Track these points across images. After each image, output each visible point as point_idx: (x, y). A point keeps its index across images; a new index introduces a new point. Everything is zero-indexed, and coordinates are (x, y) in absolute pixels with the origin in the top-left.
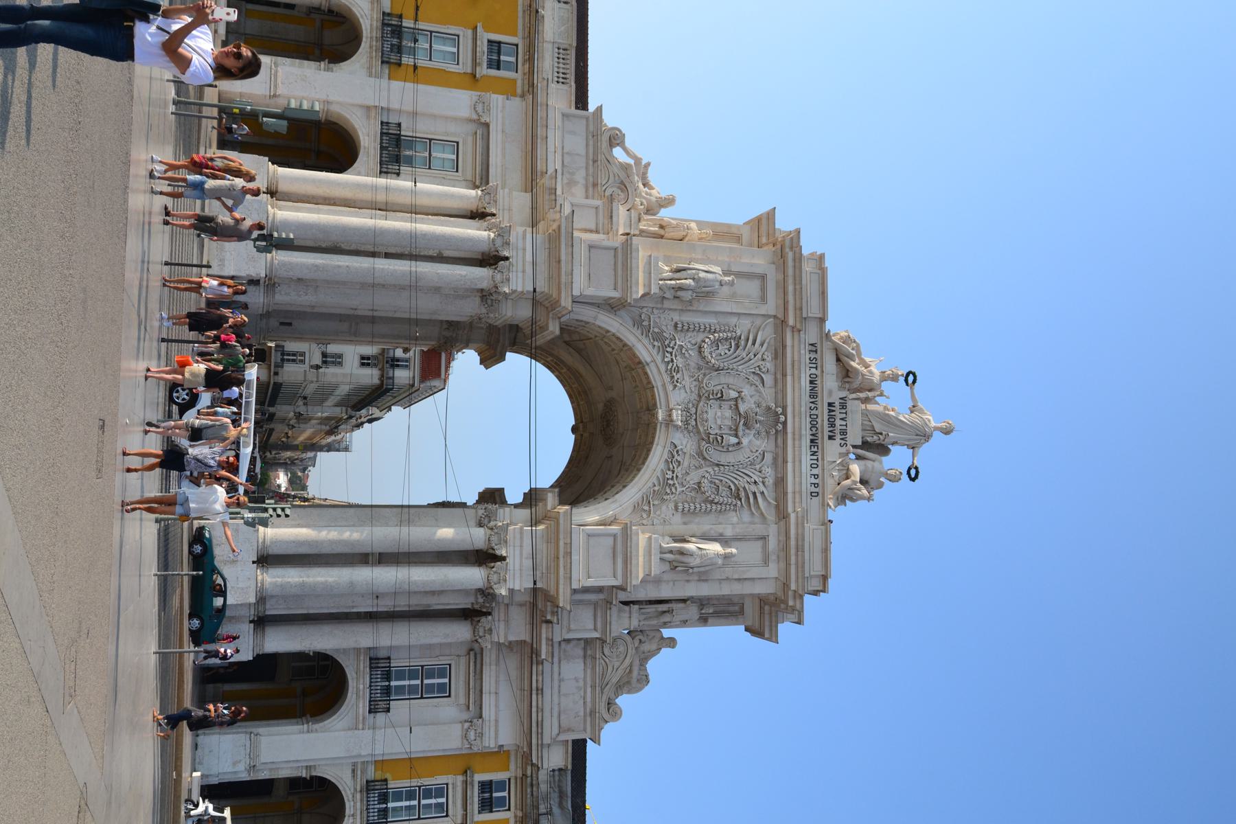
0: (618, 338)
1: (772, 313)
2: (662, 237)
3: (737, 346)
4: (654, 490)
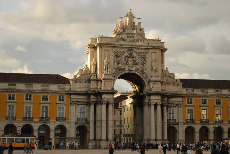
2: (96, 69)
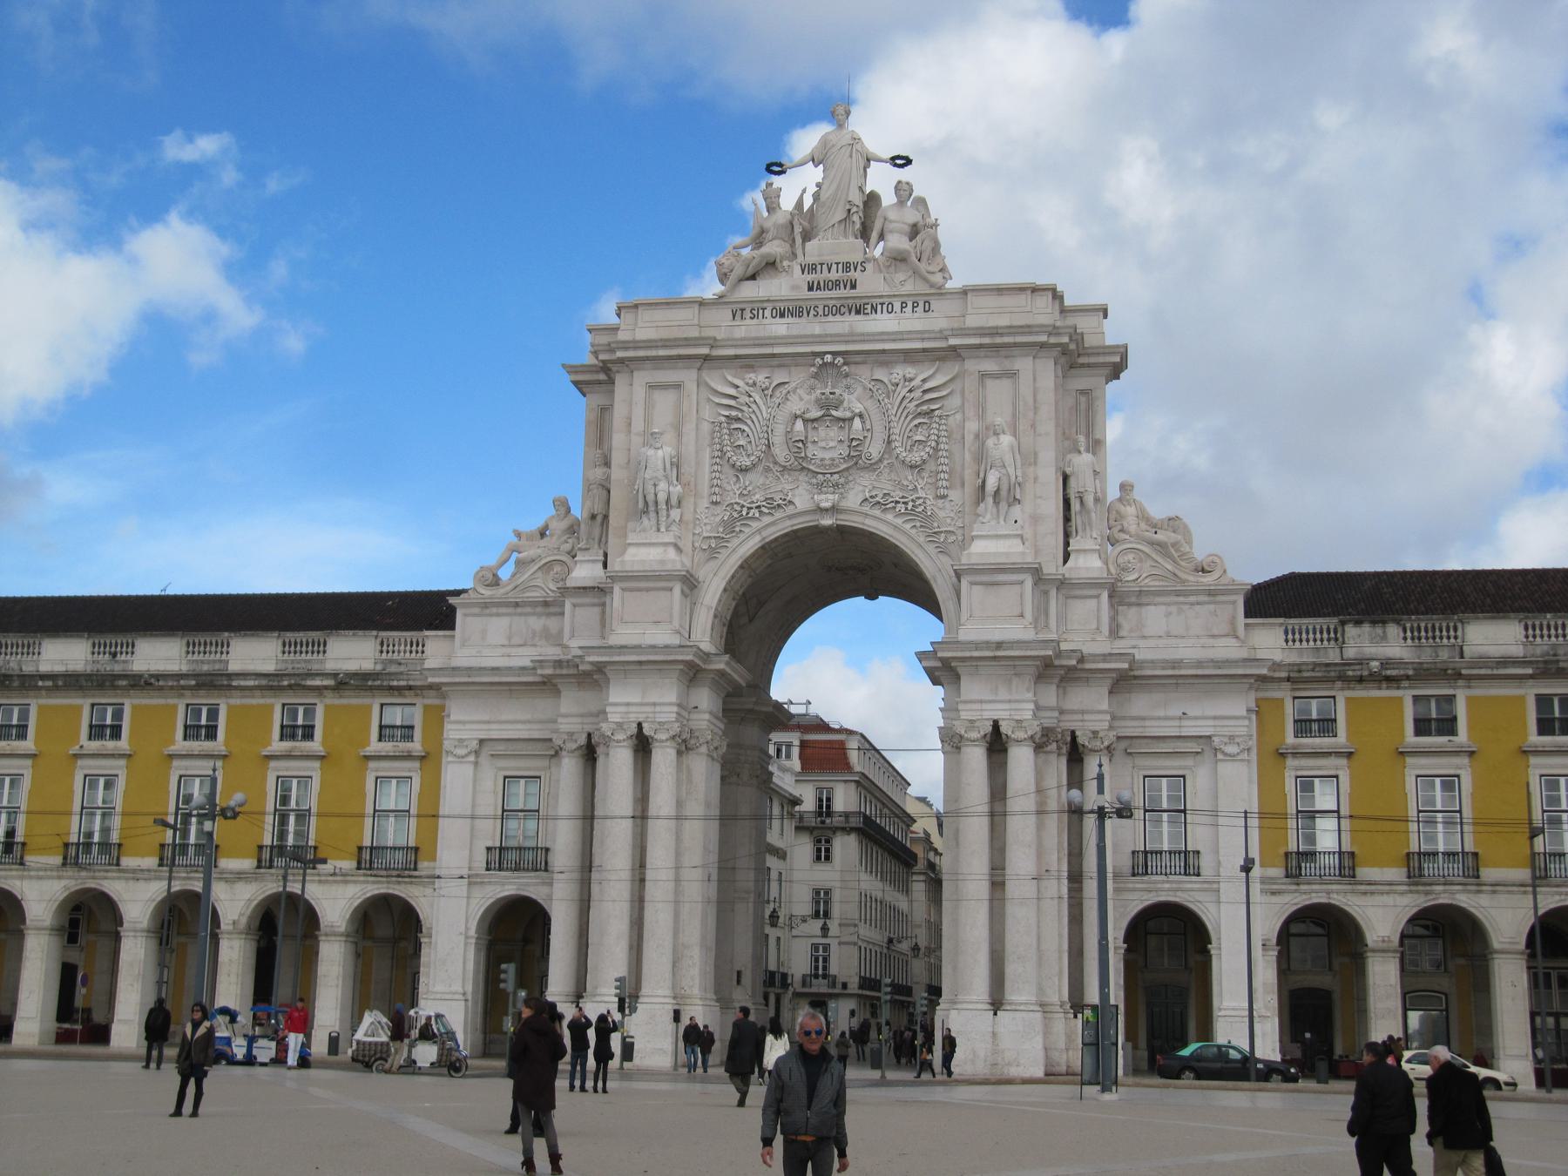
0: (733, 577)
1: (693, 374)
2: (606, 517)
3: (738, 420)
4: (921, 526)
